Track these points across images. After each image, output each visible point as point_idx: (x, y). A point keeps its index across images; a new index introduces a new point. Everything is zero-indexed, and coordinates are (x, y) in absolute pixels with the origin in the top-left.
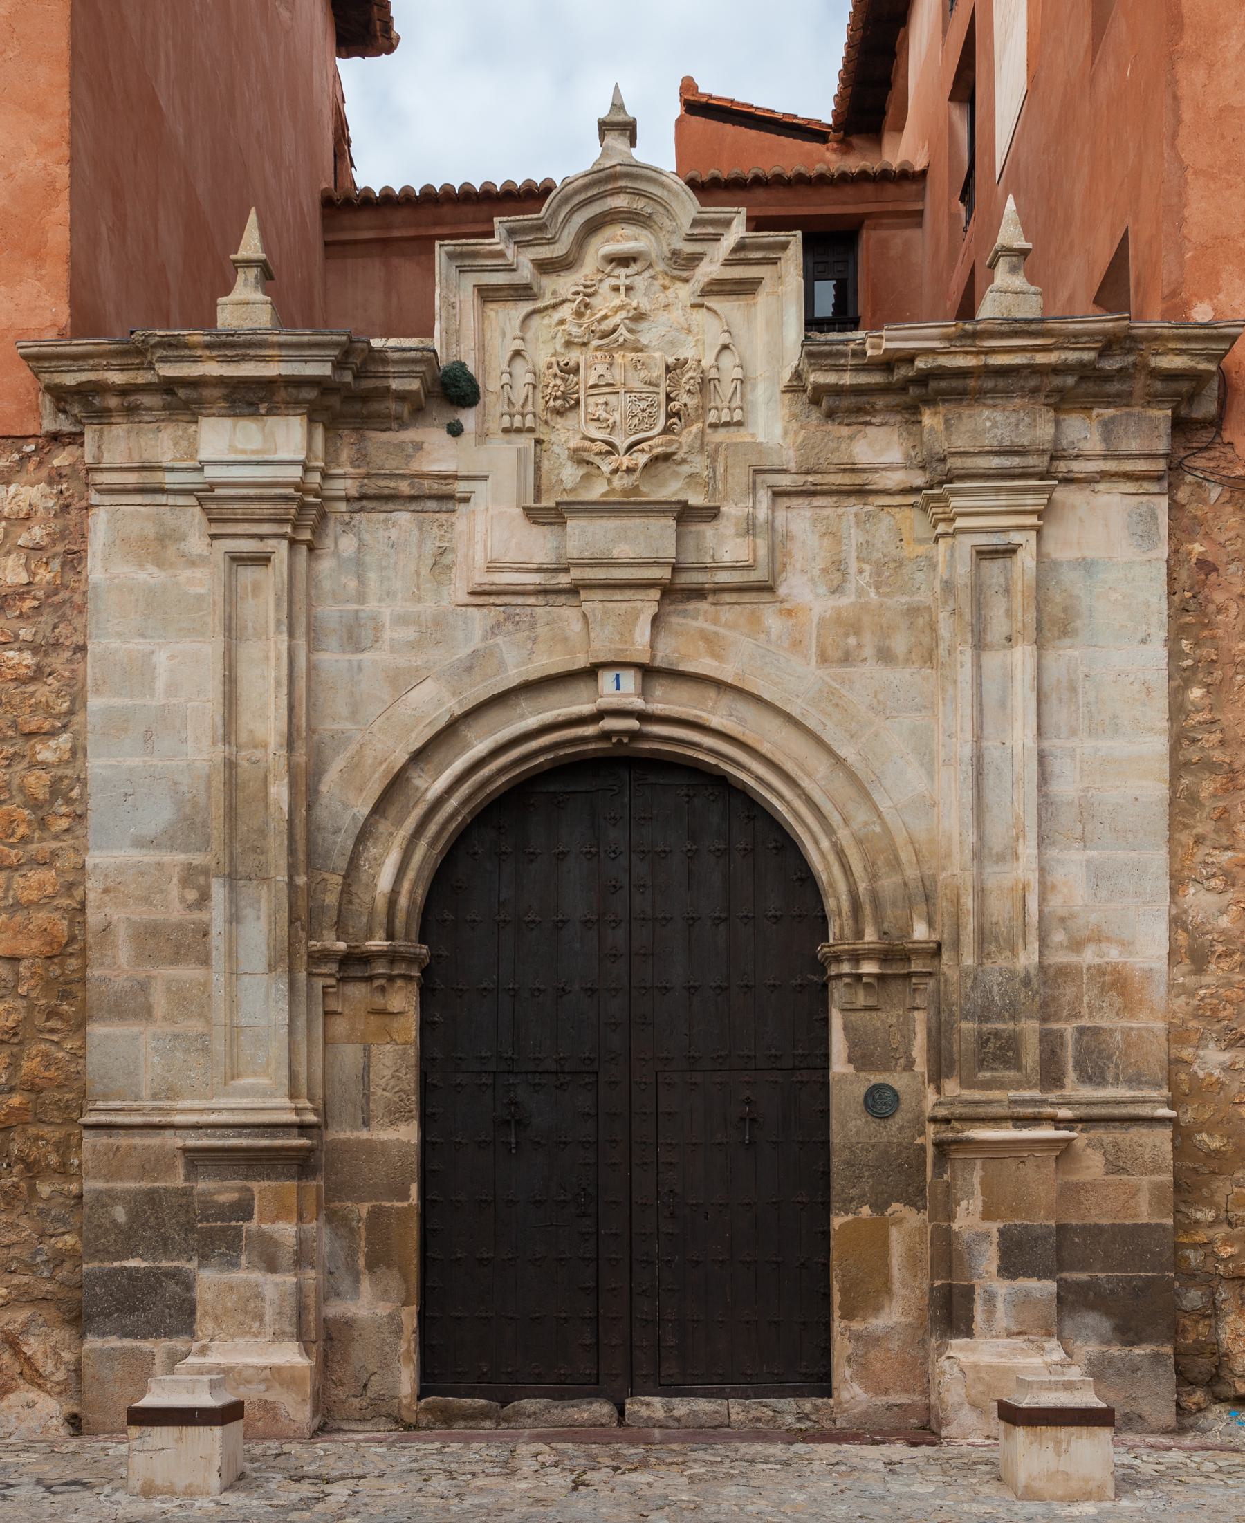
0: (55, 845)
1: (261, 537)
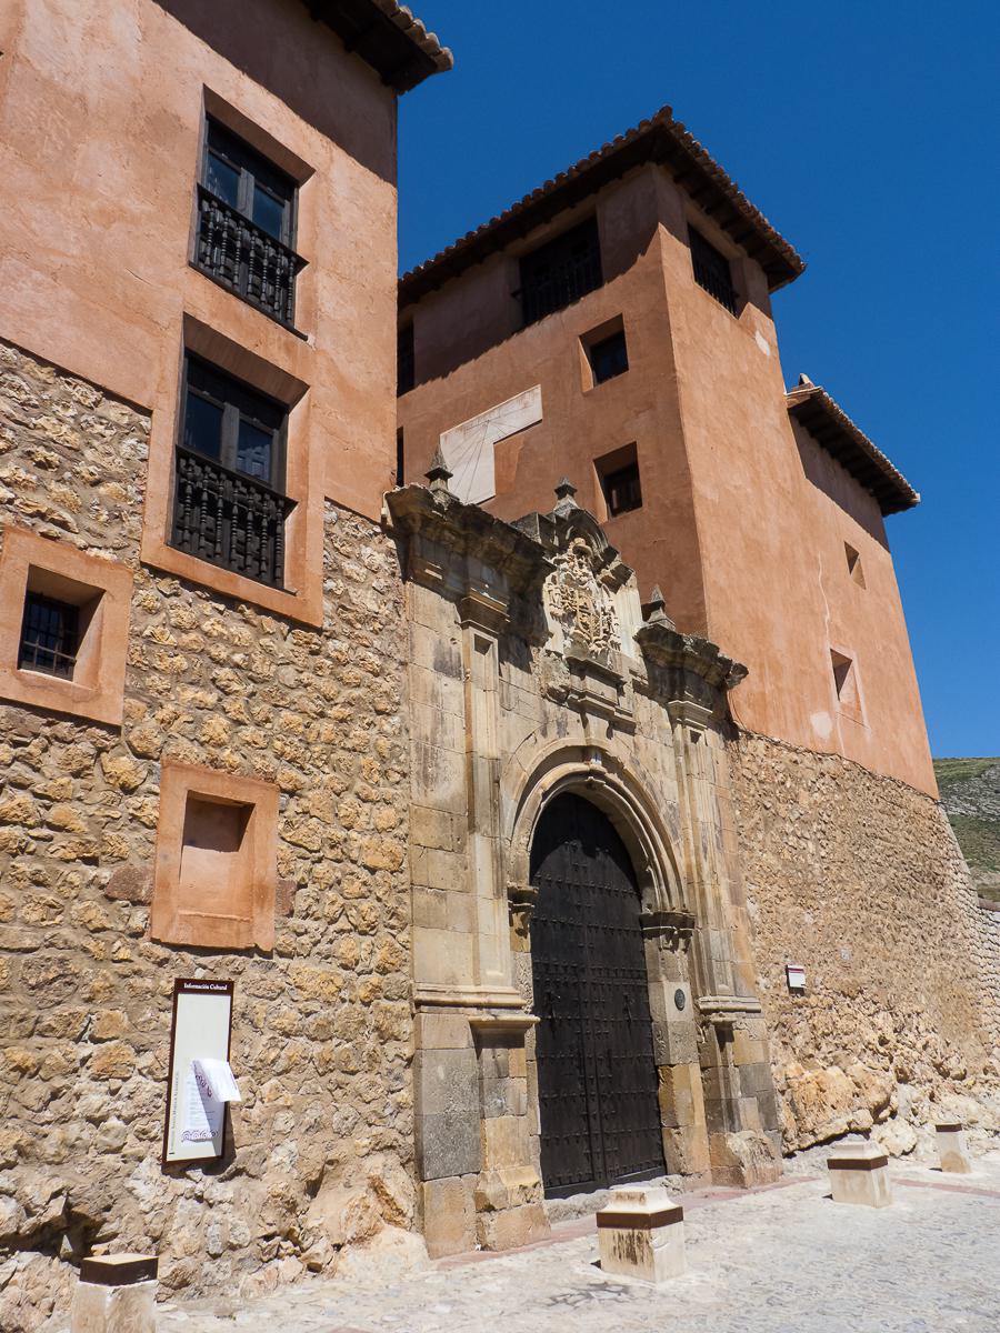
0: (392, 791)
1: (488, 632)
